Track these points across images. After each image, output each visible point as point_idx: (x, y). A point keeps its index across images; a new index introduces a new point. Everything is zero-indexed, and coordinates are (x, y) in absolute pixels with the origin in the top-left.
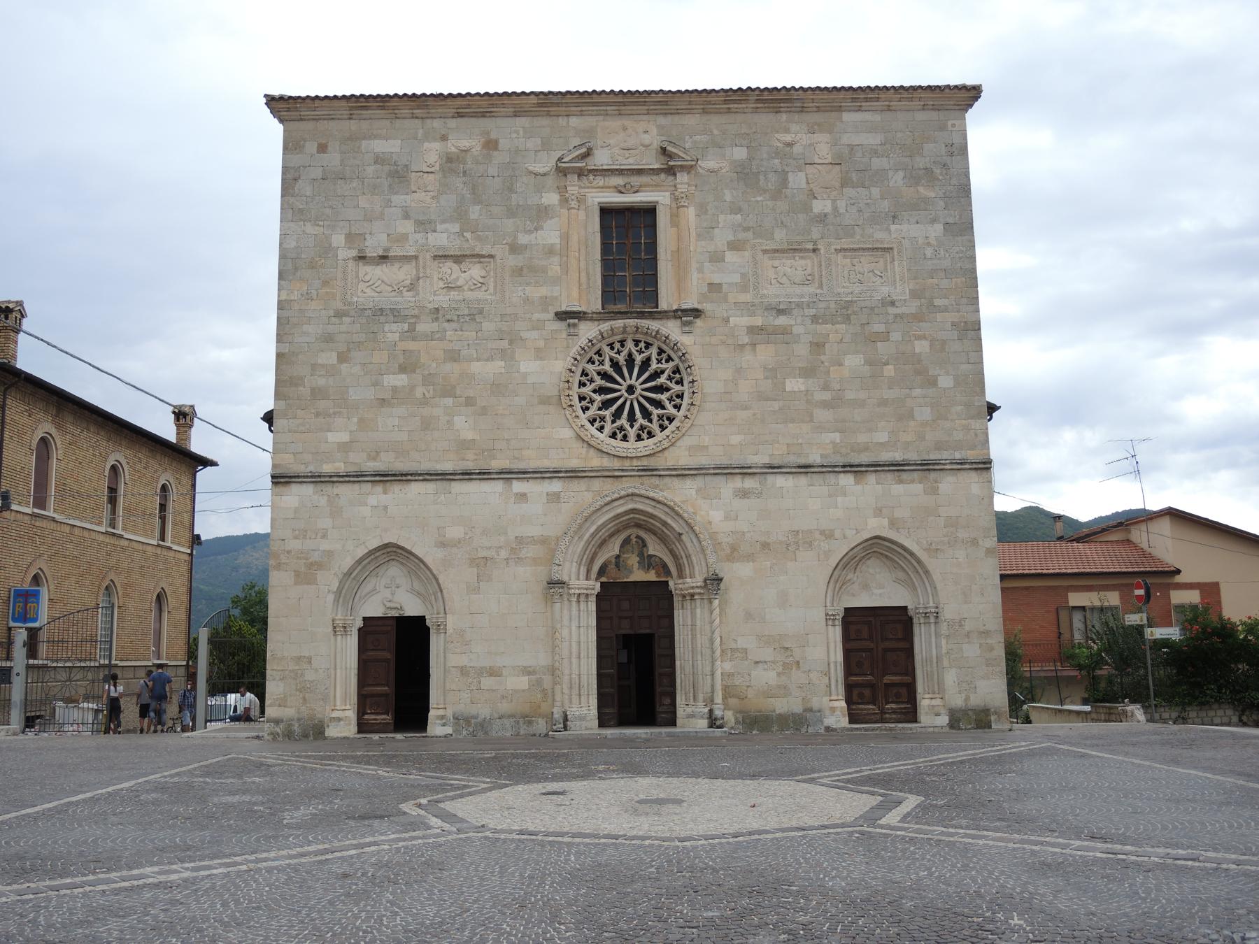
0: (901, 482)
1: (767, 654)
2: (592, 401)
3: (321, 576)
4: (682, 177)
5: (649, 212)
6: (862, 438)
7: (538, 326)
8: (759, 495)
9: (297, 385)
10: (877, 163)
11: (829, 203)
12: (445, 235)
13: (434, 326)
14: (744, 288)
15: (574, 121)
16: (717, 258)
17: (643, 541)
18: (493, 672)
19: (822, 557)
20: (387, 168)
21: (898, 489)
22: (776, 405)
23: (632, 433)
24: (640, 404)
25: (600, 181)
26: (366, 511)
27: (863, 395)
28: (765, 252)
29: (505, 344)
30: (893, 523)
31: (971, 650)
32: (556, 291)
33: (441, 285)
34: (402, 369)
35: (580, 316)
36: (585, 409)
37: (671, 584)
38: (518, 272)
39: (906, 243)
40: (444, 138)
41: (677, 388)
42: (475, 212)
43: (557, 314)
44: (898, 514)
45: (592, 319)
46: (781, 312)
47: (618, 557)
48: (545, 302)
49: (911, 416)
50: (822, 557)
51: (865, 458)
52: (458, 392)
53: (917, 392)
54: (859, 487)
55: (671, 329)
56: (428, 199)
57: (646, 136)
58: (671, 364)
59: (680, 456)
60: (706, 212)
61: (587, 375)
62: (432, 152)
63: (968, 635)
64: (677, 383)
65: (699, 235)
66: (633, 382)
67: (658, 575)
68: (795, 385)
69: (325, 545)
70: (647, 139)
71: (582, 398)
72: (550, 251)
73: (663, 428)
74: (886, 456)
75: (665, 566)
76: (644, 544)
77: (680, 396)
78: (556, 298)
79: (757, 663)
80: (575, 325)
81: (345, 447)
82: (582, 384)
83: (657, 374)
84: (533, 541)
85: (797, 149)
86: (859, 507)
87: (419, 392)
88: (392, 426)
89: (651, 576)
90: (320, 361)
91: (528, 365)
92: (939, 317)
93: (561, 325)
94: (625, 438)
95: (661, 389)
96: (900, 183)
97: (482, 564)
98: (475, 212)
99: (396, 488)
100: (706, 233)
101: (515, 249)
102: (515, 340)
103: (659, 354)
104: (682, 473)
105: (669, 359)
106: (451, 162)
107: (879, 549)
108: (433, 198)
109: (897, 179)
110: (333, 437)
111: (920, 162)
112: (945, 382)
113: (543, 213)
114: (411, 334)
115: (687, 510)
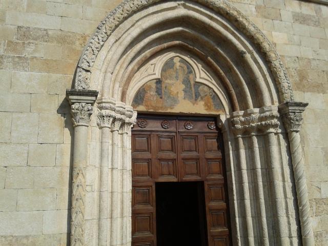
8: (317, 23)
17: (189, 66)
47: (159, 81)
76: (190, 70)
84: (45, 36)
89: (200, 108)
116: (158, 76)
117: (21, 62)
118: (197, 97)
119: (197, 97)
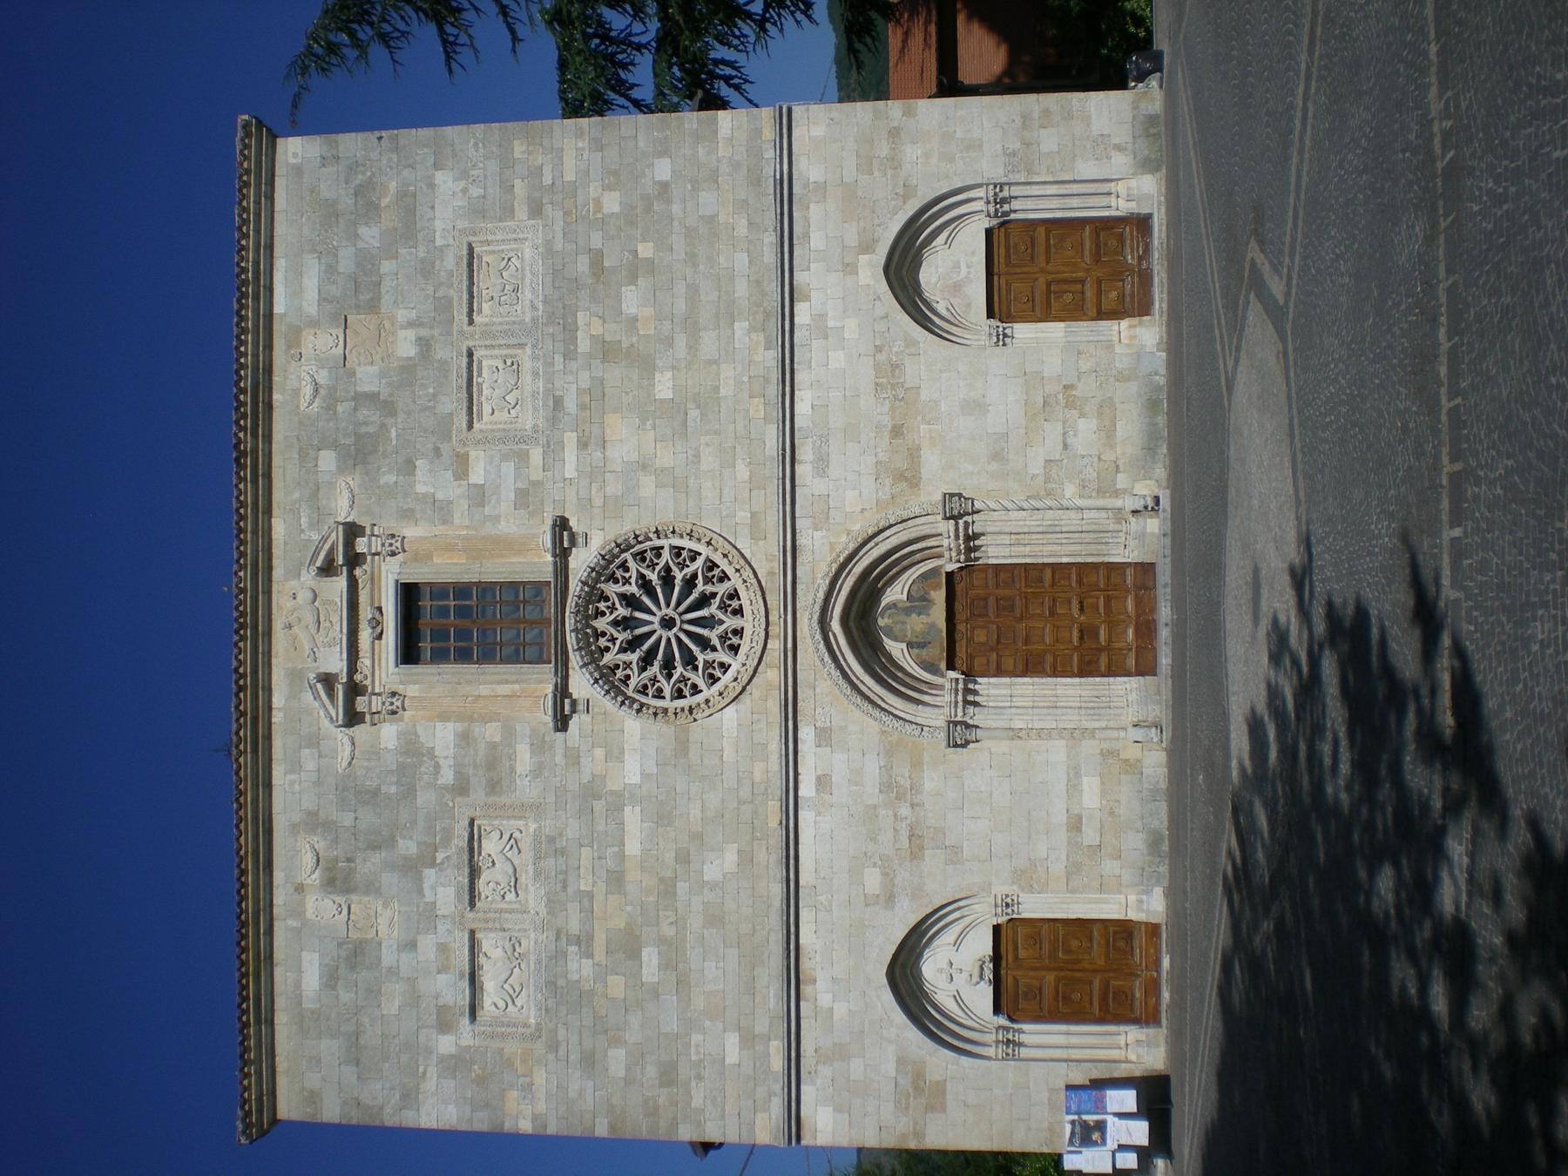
0: (807, 236)
1: (1053, 431)
2: (684, 680)
3: (933, 1075)
4: (361, 545)
5: (409, 594)
6: (742, 289)
7: (573, 757)
9: (656, 1108)
10: (346, 263)
11: (402, 334)
12: (440, 890)
13: (573, 907)
14: (523, 458)
15: (278, 700)
16: (479, 496)
18: (1075, 824)
19: (913, 350)
20: (342, 971)
21: (817, 240)
22: (694, 413)
23: (731, 622)
24: (688, 611)
25: (365, 662)
26: (840, 1010)
27: (681, 288)
28: (470, 426)
29: (599, 806)
30: (867, 247)
31: (1049, 140)
32: (522, 729)
33: (510, 897)
34: (635, 954)
35: (562, 691)
36: (696, 690)
37: (951, 567)
38: (493, 787)
39: (461, 224)
40: (300, 888)
41: (666, 554)
42: (408, 847)
43: (557, 730)
44: (852, 239)
45: (566, 678)
46: (558, 403)
47: (910, 645)
48: (539, 746)
49: (711, 220)
50: (913, 350)
51: (773, 288)
52: (669, 874)
53: (676, 209)
54: (813, 294)
55: (581, 561)
56: (389, 913)
57: (300, 597)
58: (631, 564)
59: (765, 555)
60: (412, 511)
61: (645, 687)
62: (321, 907)
63: (1028, 145)
64: (659, 556)
65: (445, 522)
66: (656, 620)
67: (936, 587)
68: (664, 387)
69: (890, 1068)
70: (304, 596)
71: (680, 695)
72: (465, 738)
73: (724, 577)
74: (770, 257)
75: (924, 576)
76: (894, 605)
77: (677, 551)
78: (533, 730)
79: (1065, 447)
80: (574, 703)
81: (749, 1039)
82: (659, 695)
83: (645, 585)
84: (887, 769)
85: (323, 377)
86: (842, 295)
87: (669, 931)
88: (714, 973)
89: (939, 596)
90: (622, 1073)
91: (632, 771)
92: (570, 176)
93: (574, 723)
94: (738, 632)
95: (667, 579)
96: (375, 231)
97: (916, 845)
98: (408, 847)
99: (805, 964)
100: (442, 511)
101: (461, 787)
102: (591, 792)
103: (616, 581)
104: (792, 552)
105: (624, 566)
106: (338, 880)
107: (902, 270)
108: (385, 906)
109: (370, 235)
110: (732, 1057)
111: (347, 202)
112: (663, 170)
113: (412, 748)
114: (584, 942)
115: (846, 544)
116: (904, 646)
117: (915, 788)
118: (925, 600)
119: (925, 600)
